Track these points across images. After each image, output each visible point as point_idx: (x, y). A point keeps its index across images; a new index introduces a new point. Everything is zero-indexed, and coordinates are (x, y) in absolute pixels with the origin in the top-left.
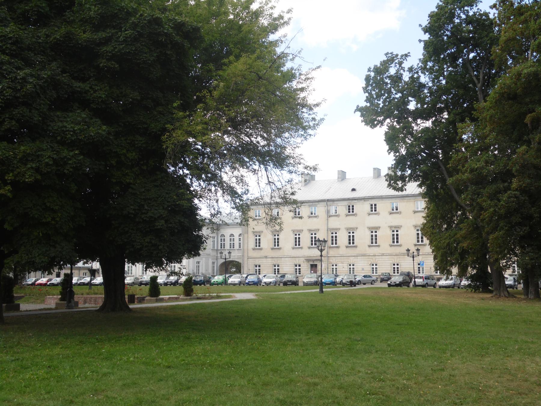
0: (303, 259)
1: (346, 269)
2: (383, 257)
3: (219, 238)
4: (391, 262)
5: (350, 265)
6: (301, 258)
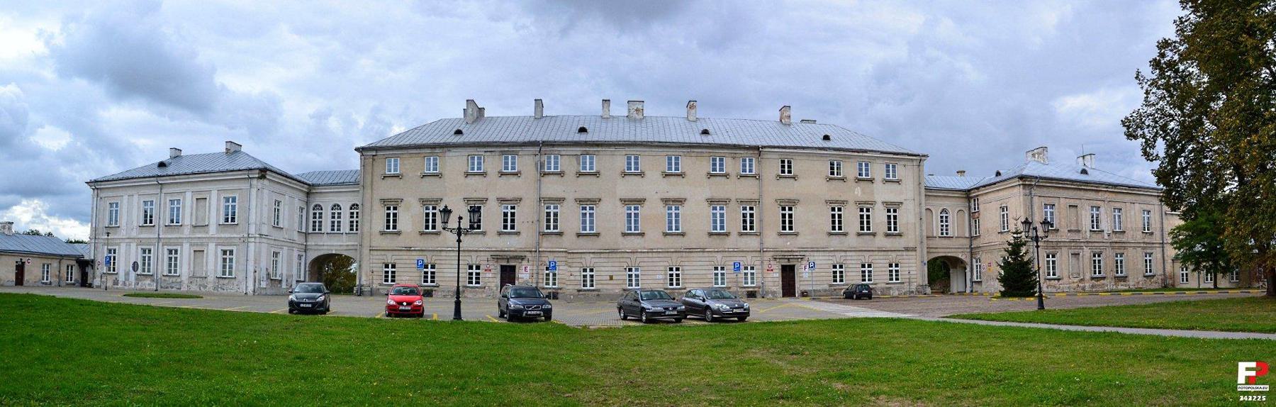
1: (578, 276)
3: (311, 212)
5: (585, 270)
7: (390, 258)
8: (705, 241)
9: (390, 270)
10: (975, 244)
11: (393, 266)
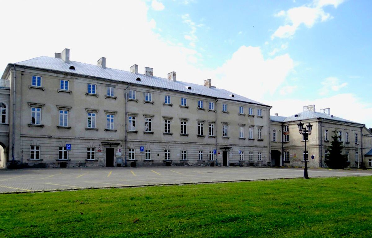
0: (99, 142)
2: (175, 145)
4: (181, 149)
6: (96, 141)
7: (35, 142)
8: (196, 139)
9: (35, 150)
10: (285, 145)
11: (38, 148)
